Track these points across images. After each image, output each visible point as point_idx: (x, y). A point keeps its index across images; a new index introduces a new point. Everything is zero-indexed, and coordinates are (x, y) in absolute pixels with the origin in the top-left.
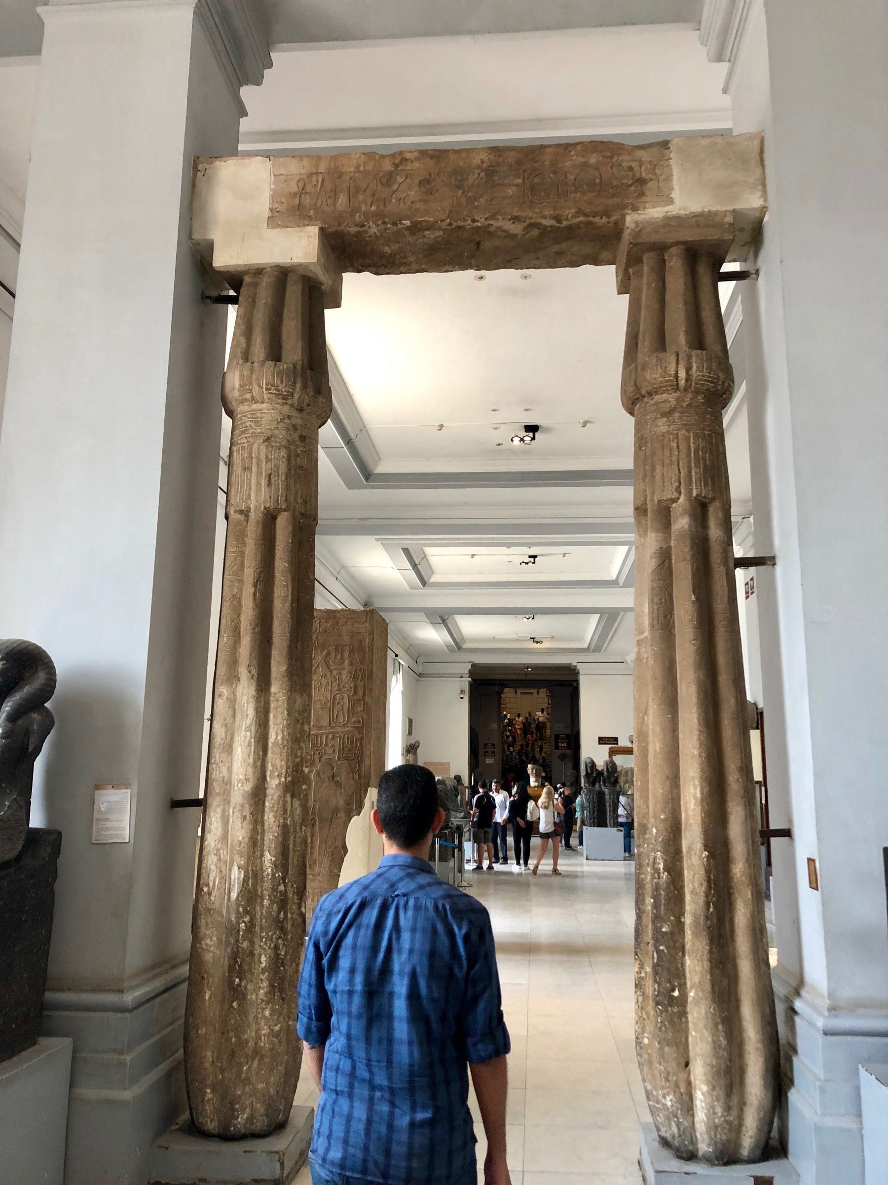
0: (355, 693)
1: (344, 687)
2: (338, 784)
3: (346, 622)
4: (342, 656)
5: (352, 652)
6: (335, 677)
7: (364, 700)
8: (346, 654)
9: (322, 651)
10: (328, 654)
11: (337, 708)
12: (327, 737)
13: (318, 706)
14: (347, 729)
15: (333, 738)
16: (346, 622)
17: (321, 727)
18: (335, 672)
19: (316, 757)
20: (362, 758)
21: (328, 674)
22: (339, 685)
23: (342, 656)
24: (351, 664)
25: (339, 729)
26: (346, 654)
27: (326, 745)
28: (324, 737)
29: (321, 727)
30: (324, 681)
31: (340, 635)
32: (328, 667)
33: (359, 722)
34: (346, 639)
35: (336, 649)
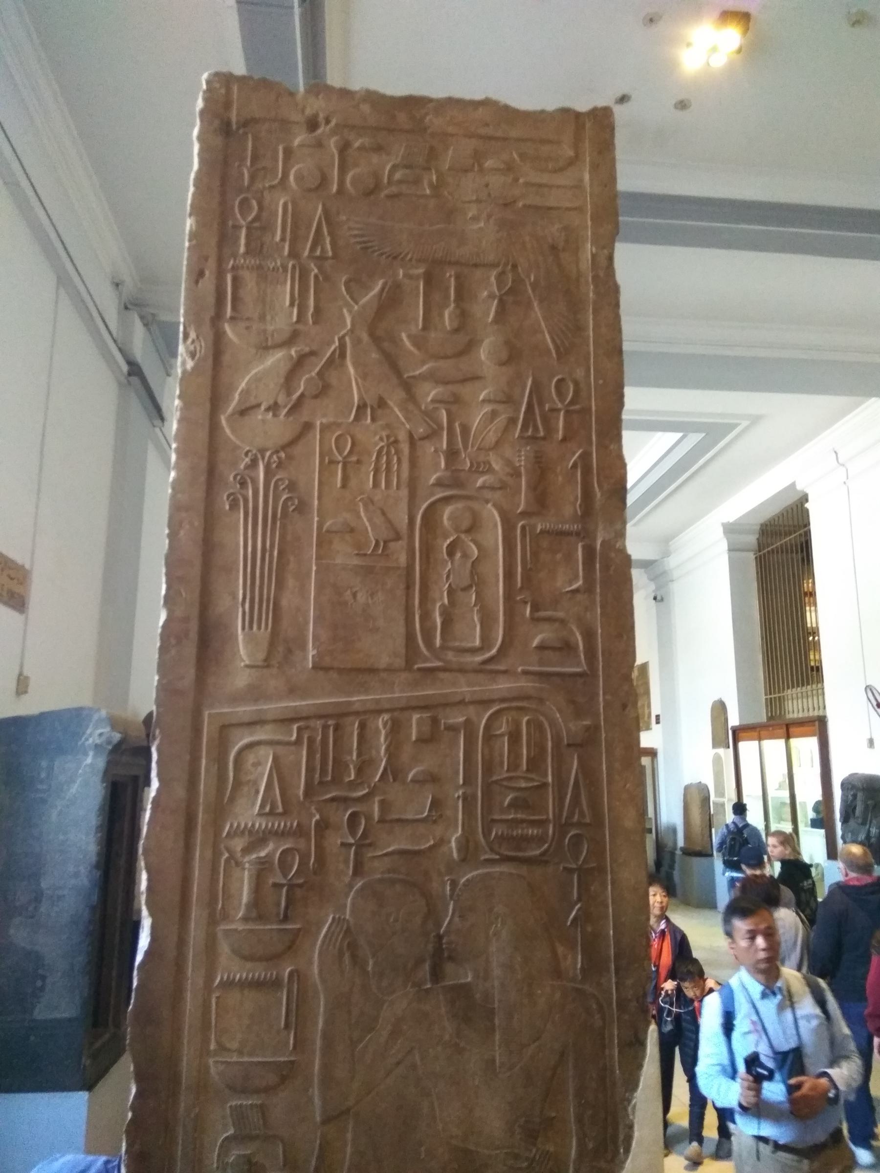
0: (541, 499)
1: (479, 468)
2: (468, 1007)
3: (478, 156)
4: (463, 315)
5: (510, 300)
6: (429, 415)
7: (585, 534)
8: (485, 309)
9: (356, 284)
10: (391, 301)
11: (448, 572)
12: (396, 728)
13: (343, 554)
14: (503, 686)
15: (428, 739)
16: (478, 156)
17: (364, 673)
18: (430, 393)
19: (334, 841)
20: (598, 851)
21: (395, 399)
22: (452, 454)
23: (463, 315)
24: (512, 355)
25: (464, 688)
26: (485, 309)
27: (394, 772)
28: (381, 722)
29: (364, 673)
30: (372, 435)
31: (450, 214)
32: (392, 362)
33: (566, 647)
34: (480, 231)
35: (429, 279)
